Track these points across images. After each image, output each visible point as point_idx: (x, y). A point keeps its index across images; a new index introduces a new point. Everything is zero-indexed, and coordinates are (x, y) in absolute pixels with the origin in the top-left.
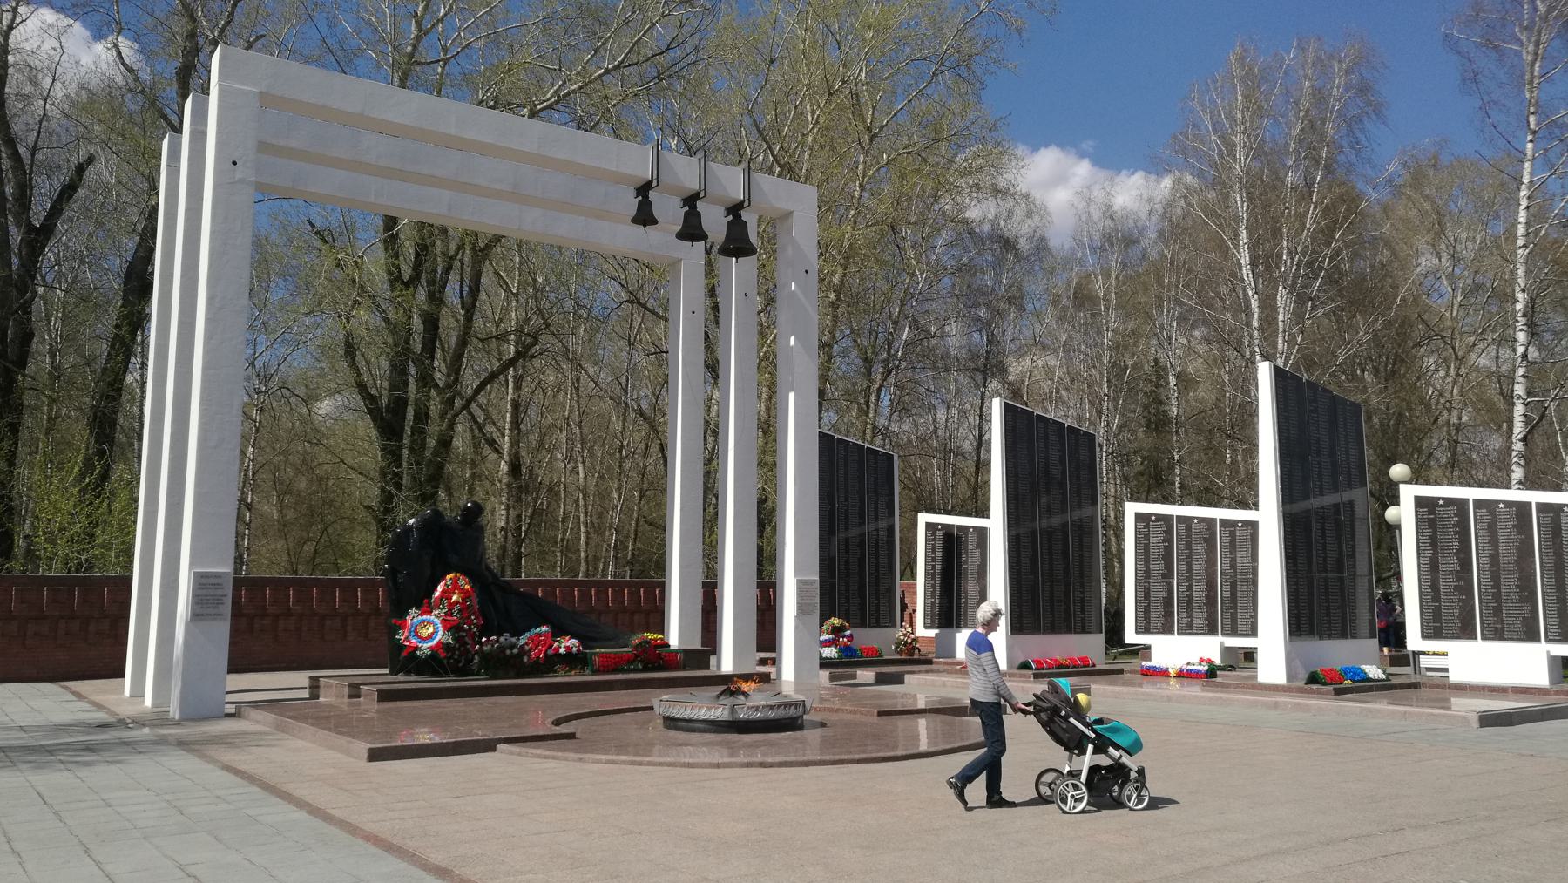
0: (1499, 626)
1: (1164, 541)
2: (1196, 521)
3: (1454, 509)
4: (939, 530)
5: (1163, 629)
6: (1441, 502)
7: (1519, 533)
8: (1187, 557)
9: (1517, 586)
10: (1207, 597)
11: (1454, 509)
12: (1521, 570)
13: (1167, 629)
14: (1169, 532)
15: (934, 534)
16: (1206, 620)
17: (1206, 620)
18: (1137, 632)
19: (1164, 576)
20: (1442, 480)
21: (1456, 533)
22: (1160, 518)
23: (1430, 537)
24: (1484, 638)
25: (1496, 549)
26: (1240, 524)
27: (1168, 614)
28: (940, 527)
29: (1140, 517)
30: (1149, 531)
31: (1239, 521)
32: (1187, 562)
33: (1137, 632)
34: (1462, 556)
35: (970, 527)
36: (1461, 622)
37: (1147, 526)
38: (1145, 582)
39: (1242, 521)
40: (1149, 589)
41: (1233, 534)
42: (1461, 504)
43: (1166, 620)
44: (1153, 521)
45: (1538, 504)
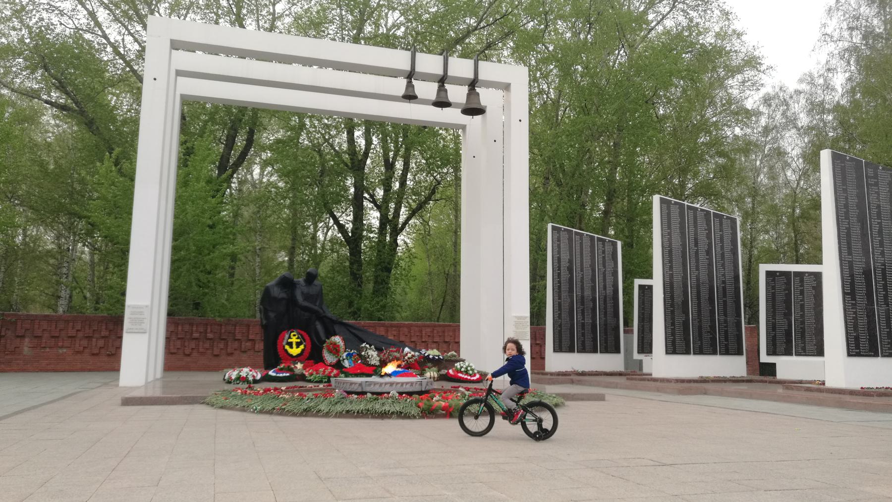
1: (785, 290)
2: (807, 275)
5: (785, 351)
8: (801, 301)
13: (788, 353)
14: (788, 283)
15: (643, 292)
16: (815, 345)
17: (815, 345)
27: (789, 341)
29: (769, 274)
30: (775, 283)
37: (774, 280)
38: (773, 319)
44: (777, 276)
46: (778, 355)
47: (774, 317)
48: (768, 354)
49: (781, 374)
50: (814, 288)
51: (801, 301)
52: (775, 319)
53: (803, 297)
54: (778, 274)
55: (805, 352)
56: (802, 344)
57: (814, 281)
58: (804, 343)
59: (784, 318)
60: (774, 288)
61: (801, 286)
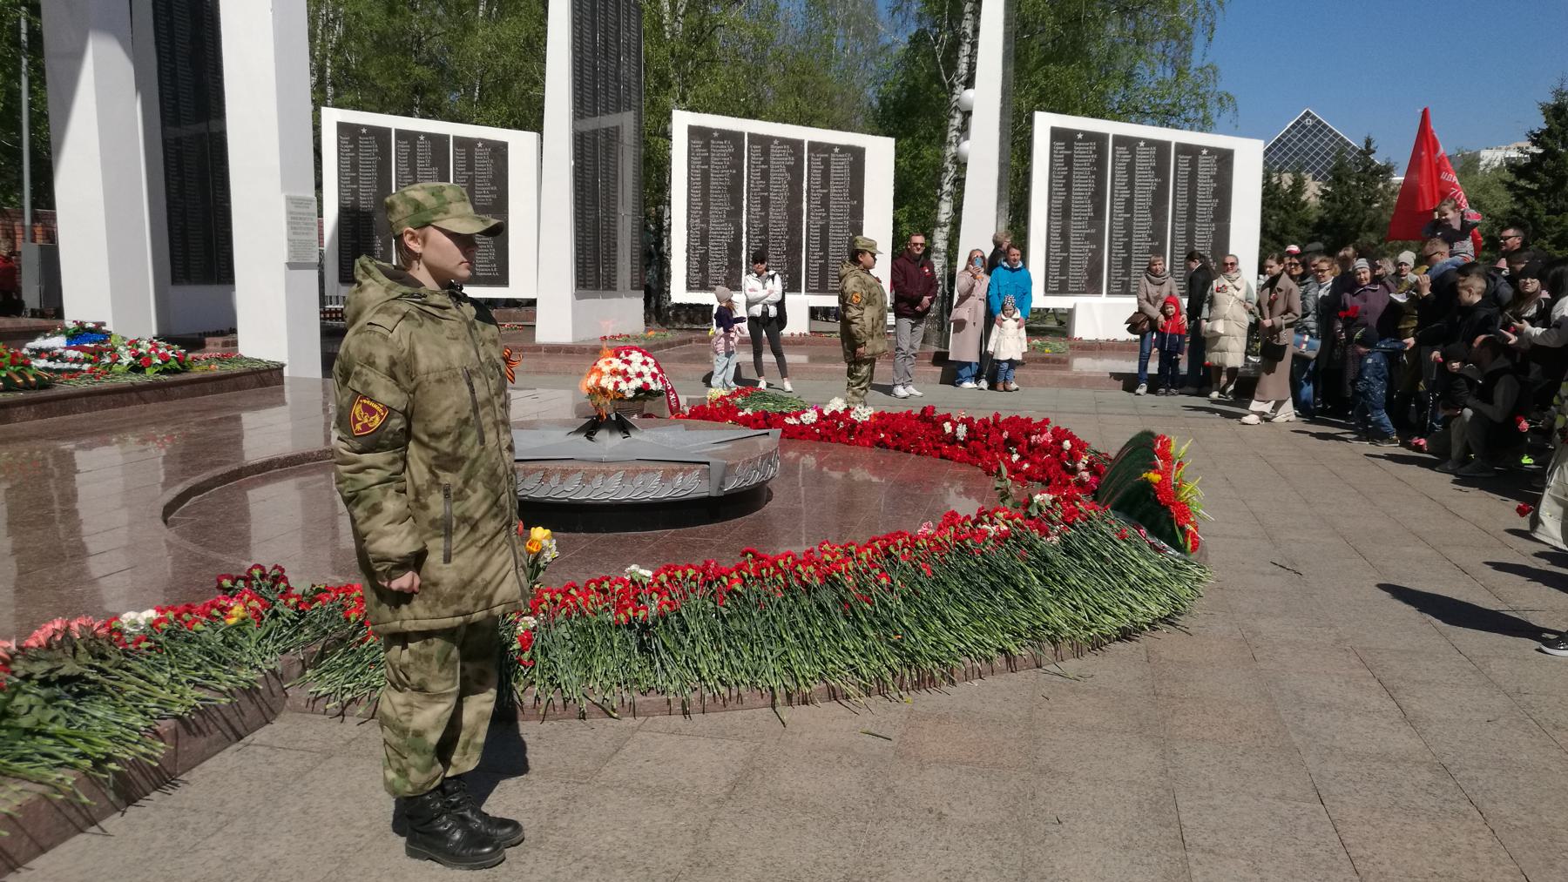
0: (1126, 279)
3: (1093, 145)
4: (364, 135)
7: (1156, 176)
8: (763, 190)
9: (1149, 235)
11: (1093, 145)
12: (1155, 217)
14: (738, 155)
17: (786, 273)
18: (690, 288)
19: (729, 214)
20: (1075, 106)
21: (1092, 173)
23: (1065, 177)
25: (1132, 194)
26: (836, 150)
28: (364, 131)
30: (709, 152)
31: (834, 146)
32: (762, 197)
33: (690, 288)
34: (1097, 200)
35: (1140, 139)
37: (707, 146)
39: (839, 146)
41: (826, 162)
42: (1100, 139)
44: (716, 139)
45: (1178, 145)
47: (705, 218)
48: (690, 288)
50: (789, 169)
52: (708, 223)
53: (768, 185)
54: (716, 134)
60: (706, 161)
61: (763, 163)
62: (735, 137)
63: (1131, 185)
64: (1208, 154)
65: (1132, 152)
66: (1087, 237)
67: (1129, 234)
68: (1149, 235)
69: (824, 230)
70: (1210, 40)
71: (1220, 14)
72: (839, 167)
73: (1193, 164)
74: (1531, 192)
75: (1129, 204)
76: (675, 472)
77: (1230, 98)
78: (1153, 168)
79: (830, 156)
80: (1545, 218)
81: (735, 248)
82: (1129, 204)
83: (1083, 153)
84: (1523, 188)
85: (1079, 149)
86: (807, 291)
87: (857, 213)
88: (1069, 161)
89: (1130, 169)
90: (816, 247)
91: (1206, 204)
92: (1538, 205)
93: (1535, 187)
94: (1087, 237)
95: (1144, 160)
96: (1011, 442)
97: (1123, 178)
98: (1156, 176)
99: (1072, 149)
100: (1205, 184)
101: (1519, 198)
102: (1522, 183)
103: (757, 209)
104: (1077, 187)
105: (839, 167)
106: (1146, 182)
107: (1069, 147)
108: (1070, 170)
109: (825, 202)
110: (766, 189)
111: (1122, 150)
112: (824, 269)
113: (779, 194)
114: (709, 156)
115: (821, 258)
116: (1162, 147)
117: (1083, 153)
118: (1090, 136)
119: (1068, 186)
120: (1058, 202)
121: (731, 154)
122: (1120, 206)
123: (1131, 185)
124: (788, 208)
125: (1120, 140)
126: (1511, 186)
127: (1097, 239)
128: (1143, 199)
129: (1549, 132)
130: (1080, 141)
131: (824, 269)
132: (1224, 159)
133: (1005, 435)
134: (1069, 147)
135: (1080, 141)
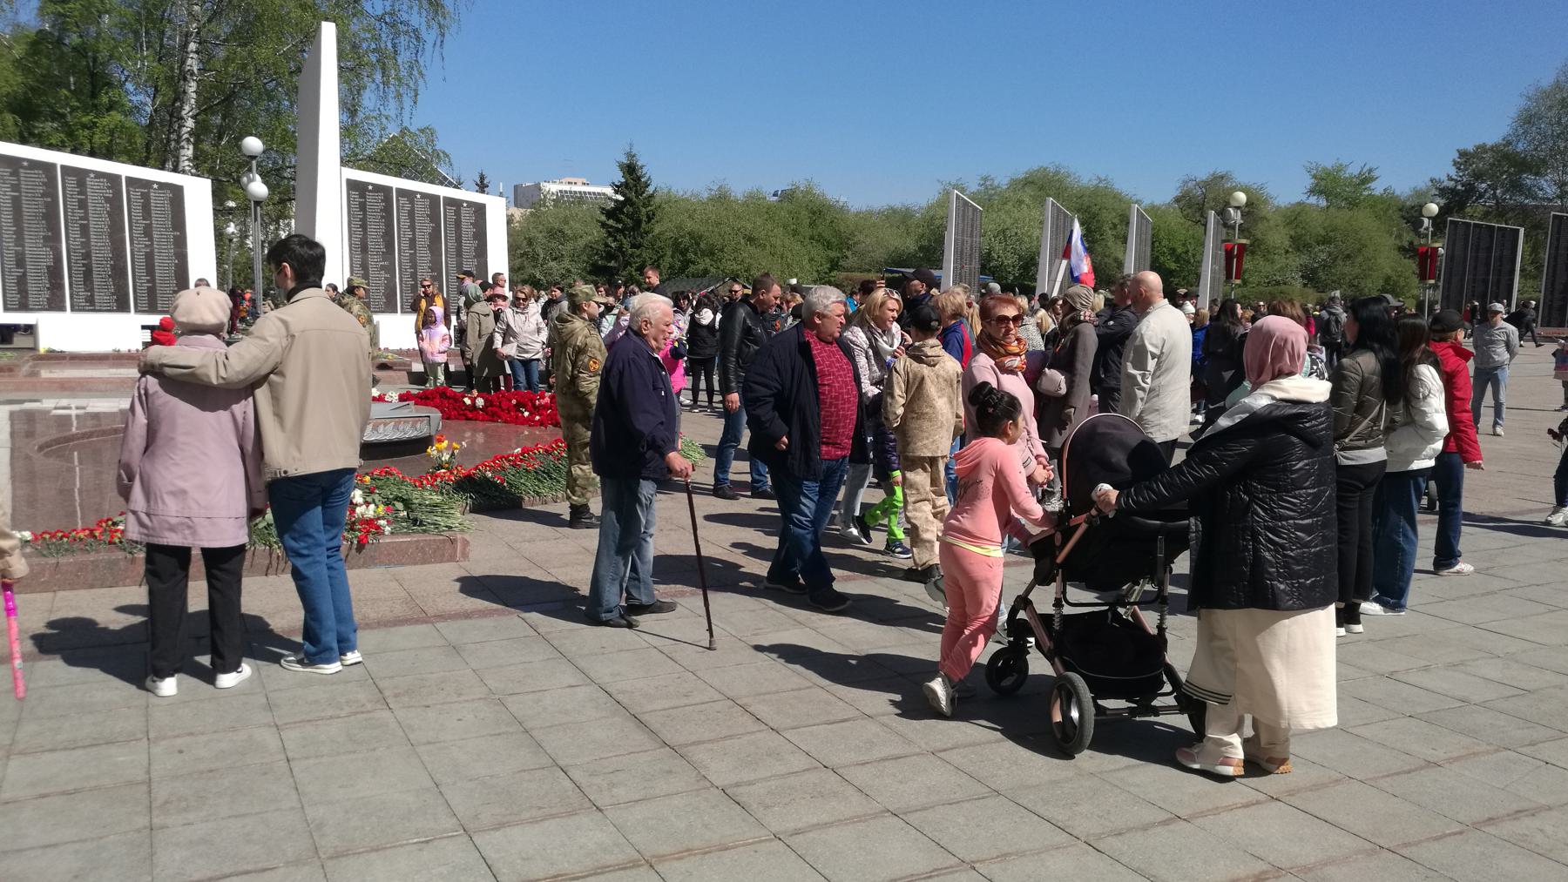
1: (43, 195)
5: (49, 304)
6: (370, 187)
7: (431, 222)
8: (81, 219)
9: (429, 267)
10: (113, 267)
11: (381, 196)
13: (55, 305)
16: (113, 294)
17: (113, 294)
21: (382, 217)
22: (34, 165)
24: (403, 312)
25: (414, 234)
27: (56, 286)
30: (19, 180)
31: (154, 182)
32: (81, 224)
36: (386, 298)
40: (23, 254)
41: (146, 197)
43: (53, 294)
44: (25, 168)
45: (445, 198)
46: (32, 310)
49: (45, 344)
50: (107, 200)
51: (81, 219)
52: (23, 246)
53: (86, 213)
55: (94, 305)
56: (86, 291)
57: (109, 188)
58: (92, 290)
59: (44, 246)
62: (48, 168)
63: (412, 228)
64: (468, 207)
65: (412, 202)
66: (382, 268)
67: (414, 266)
68: (429, 267)
69: (149, 257)
70: (415, 103)
71: (421, 81)
72: (159, 201)
73: (458, 213)
74: (617, 230)
75: (413, 242)
76: (417, 422)
77: (447, 155)
78: (428, 215)
79: (149, 192)
80: (630, 251)
81: (55, 273)
82: (413, 242)
83: (375, 202)
84: (611, 227)
85: (370, 198)
86: (137, 311)
87: (180, 243)
88: (363, 207)
89: (411, 214)
90: (142, 271)
91: (469, 245)
92: (624, 241)
93: (620, 226)
94: (382, 268)
95: (422, 209)
96: (518, 405)
97: (406, 223)
98: (431, 222)
99: (365, 198)
100: (468, 230)
101: (610, 234)
102: (611, 222)
103: (76, 234)
104: (371, 228)
105: (159, 201)
106: (424, 227)
107: (362, 195)
108: (365, 214)
109: (148, 232)
110: (86, 218)
111: (403, 200)
112: (152, 292)
113: (98, 223)
114: (19, 185)
115: (148, 281)
116: (434, 199)
117: (375, 202)
118: (378, 188)
119: (364, 226)
120: (357, 241)
121: (44, 184)
122: (405, 245)
123: (412, 228)
124: (111, 235)
125: (401, 192)
126: (603, 225)
127: (390, 270)
128: (423, 240)
129: (626, 185)
130: (370, 191)
131: (152, 292)
132: (480, 210)
133: (514, 402)
134: (362, 195)
135: (370, 191)
